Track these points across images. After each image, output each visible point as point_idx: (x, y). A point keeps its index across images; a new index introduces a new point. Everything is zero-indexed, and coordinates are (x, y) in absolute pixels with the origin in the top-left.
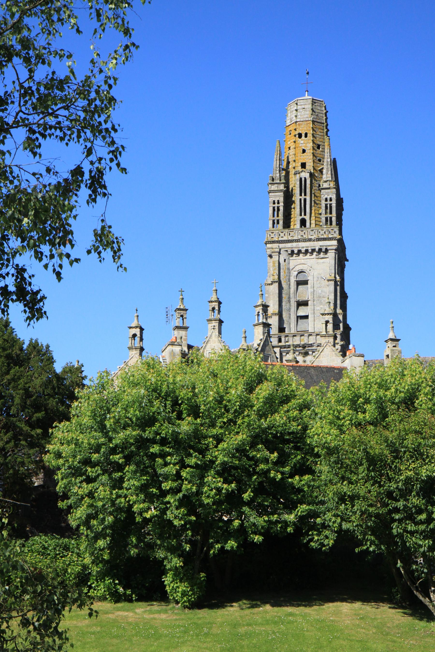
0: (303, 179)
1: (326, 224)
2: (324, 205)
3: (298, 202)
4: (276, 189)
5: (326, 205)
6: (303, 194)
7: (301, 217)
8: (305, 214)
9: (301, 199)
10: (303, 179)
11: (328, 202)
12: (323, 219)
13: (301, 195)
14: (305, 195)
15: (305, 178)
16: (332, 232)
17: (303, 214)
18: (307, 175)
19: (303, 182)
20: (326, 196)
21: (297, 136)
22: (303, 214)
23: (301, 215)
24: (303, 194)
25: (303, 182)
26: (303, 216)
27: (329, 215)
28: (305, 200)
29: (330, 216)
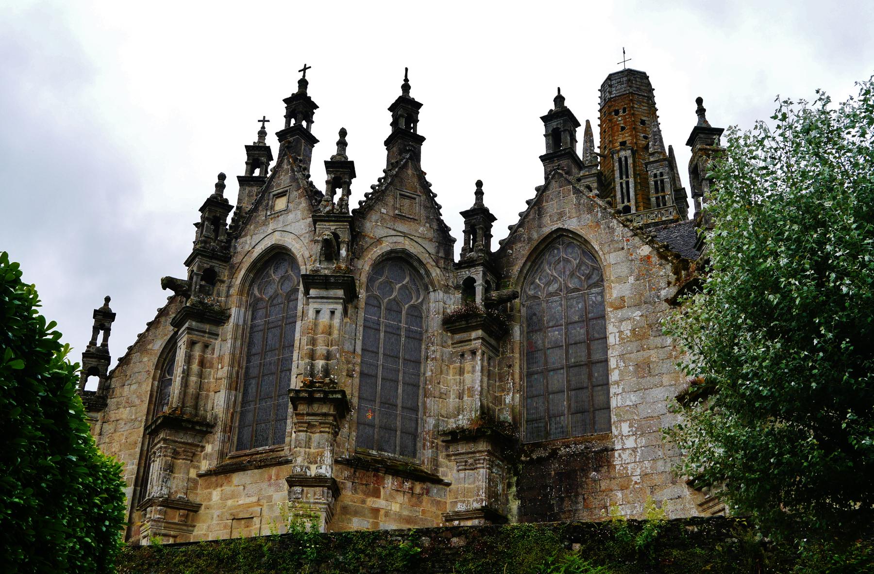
0: (623, 159)
1: (658, 205)
2: (653, 183)
3: (618, 188)
4: (587, 173)
5: (656, 182)
6: (624, 177)
8: (629, 201)
9: (621, 184)
10: (623, 159)
11: (659, 178)
12: (653, 200)
13: (621, 178)
14: (627, 177)
15: (626, 158)
17: (626, 201)
20: (655, 171)
21: (613, 113)
22: (626, 201)
23: (623, 202)
24: (624, 177)
26: (626, 203)
27: (660, 194)
28: (627, 183)
29: (662, 194)
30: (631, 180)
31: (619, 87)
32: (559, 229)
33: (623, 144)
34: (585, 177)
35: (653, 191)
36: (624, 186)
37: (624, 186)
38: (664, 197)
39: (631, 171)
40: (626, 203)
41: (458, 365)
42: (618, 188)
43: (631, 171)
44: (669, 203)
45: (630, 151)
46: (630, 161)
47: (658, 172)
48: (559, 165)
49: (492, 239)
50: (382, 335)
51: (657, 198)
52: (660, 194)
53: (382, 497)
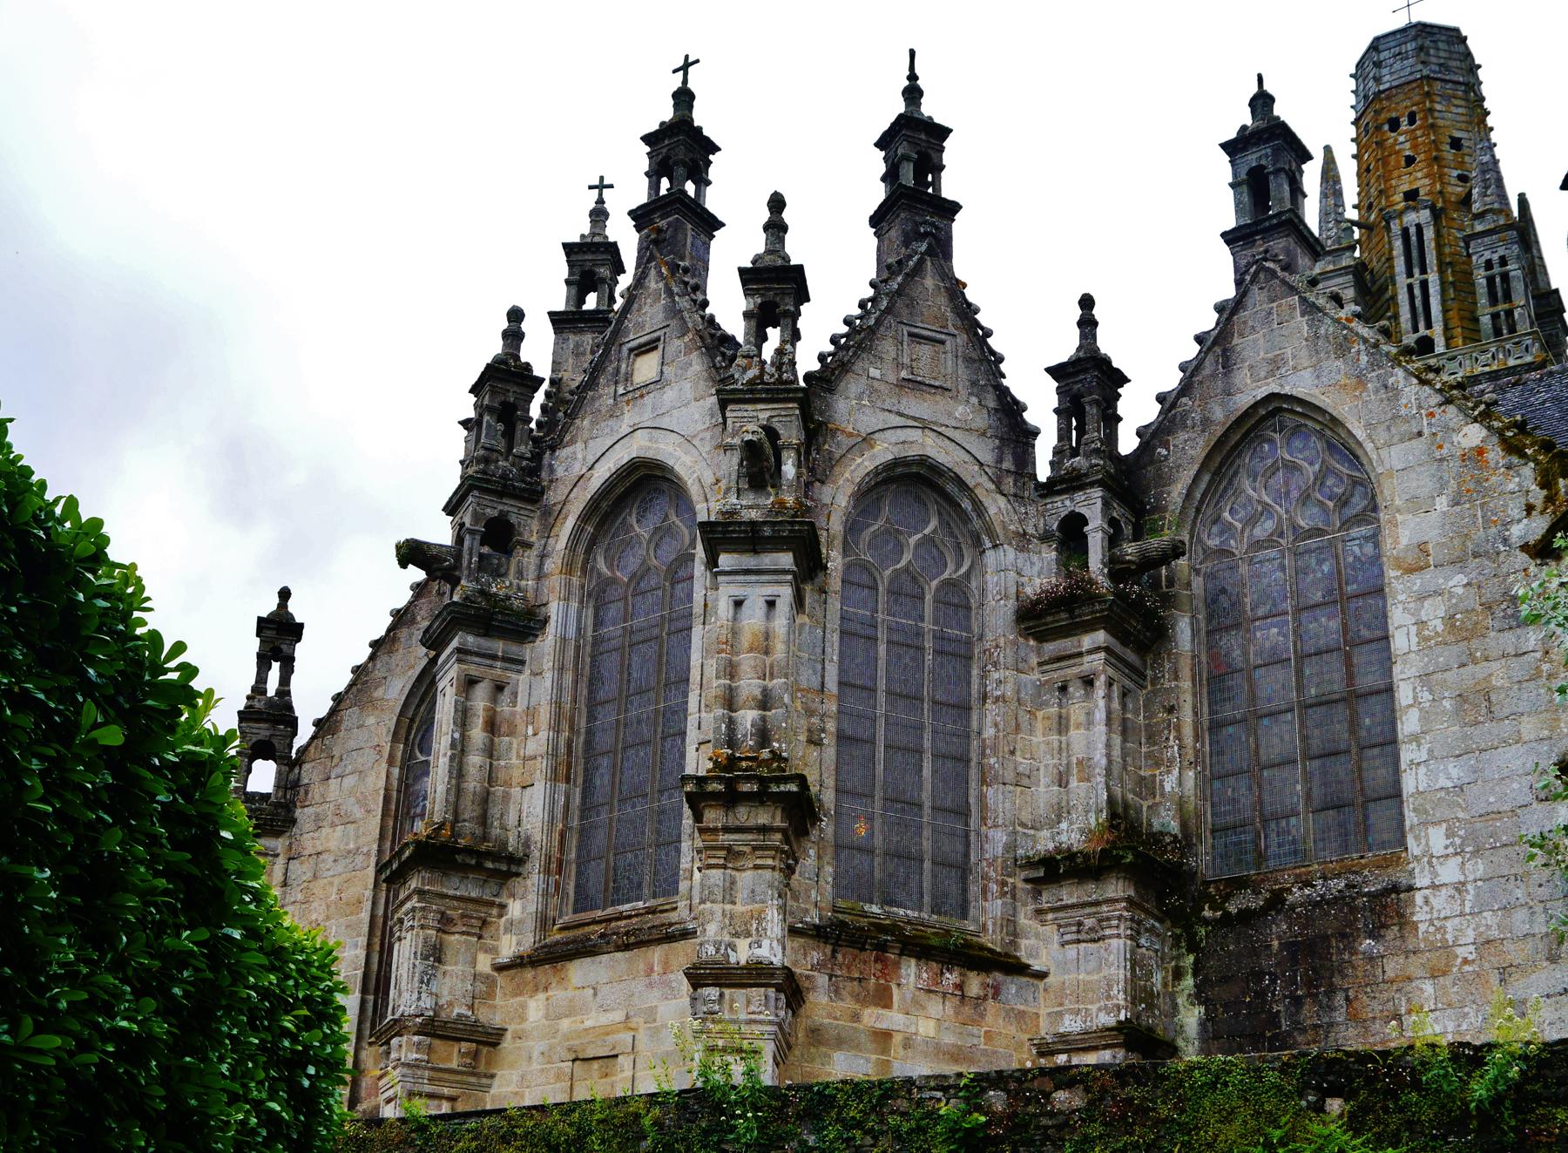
0: (1413, 230)
1: (1497, 332)
2: (1484, 282)
3: (1403, 297)
4: (1331, 267)
5: (1490, 281)
6: (1416, 271)
7: (1416, 336)
8: (1429, 326)
9: (1410, 287)
10: (1413, 230)
11: (1497, 270)
12: (1486, 320)
13: (1410, 274)
14: (1424, 271)
15: (1419, 227)
16: (1518, 352)
17: (1421, 325)
18: (1424, 216)
19: (1414, 239)
20: (1487, 255)
21: (1386, 127)
22: (1421, 325)
23: (1416, 330)
24: (1416, 271)
25: (1414, 239)
28: (1424, 285)
29: (1506, 306)
30: (1433, 278)
31: (1397, 66)
32: (1272, 397)
33: (1411, 195)
34: (1325, 275)
35: (1483, 300)
36: (1417, 291)
37: (1417, 291)
38: (1510, 313)
39: (1431, 258)
40: (1423, 331)
41: (1054, 710)
42: (1403, 297)
43: (1431, 258)
44: (1523, 327)
45: (1427, 212)
46: (1429, 234)
47: (1495, 257)
48: (1266, 251)
49: (1121, 426)
50: (882, 649)
51: (1495, 316)
52: (1501, 307)
53: (895, 1005)
